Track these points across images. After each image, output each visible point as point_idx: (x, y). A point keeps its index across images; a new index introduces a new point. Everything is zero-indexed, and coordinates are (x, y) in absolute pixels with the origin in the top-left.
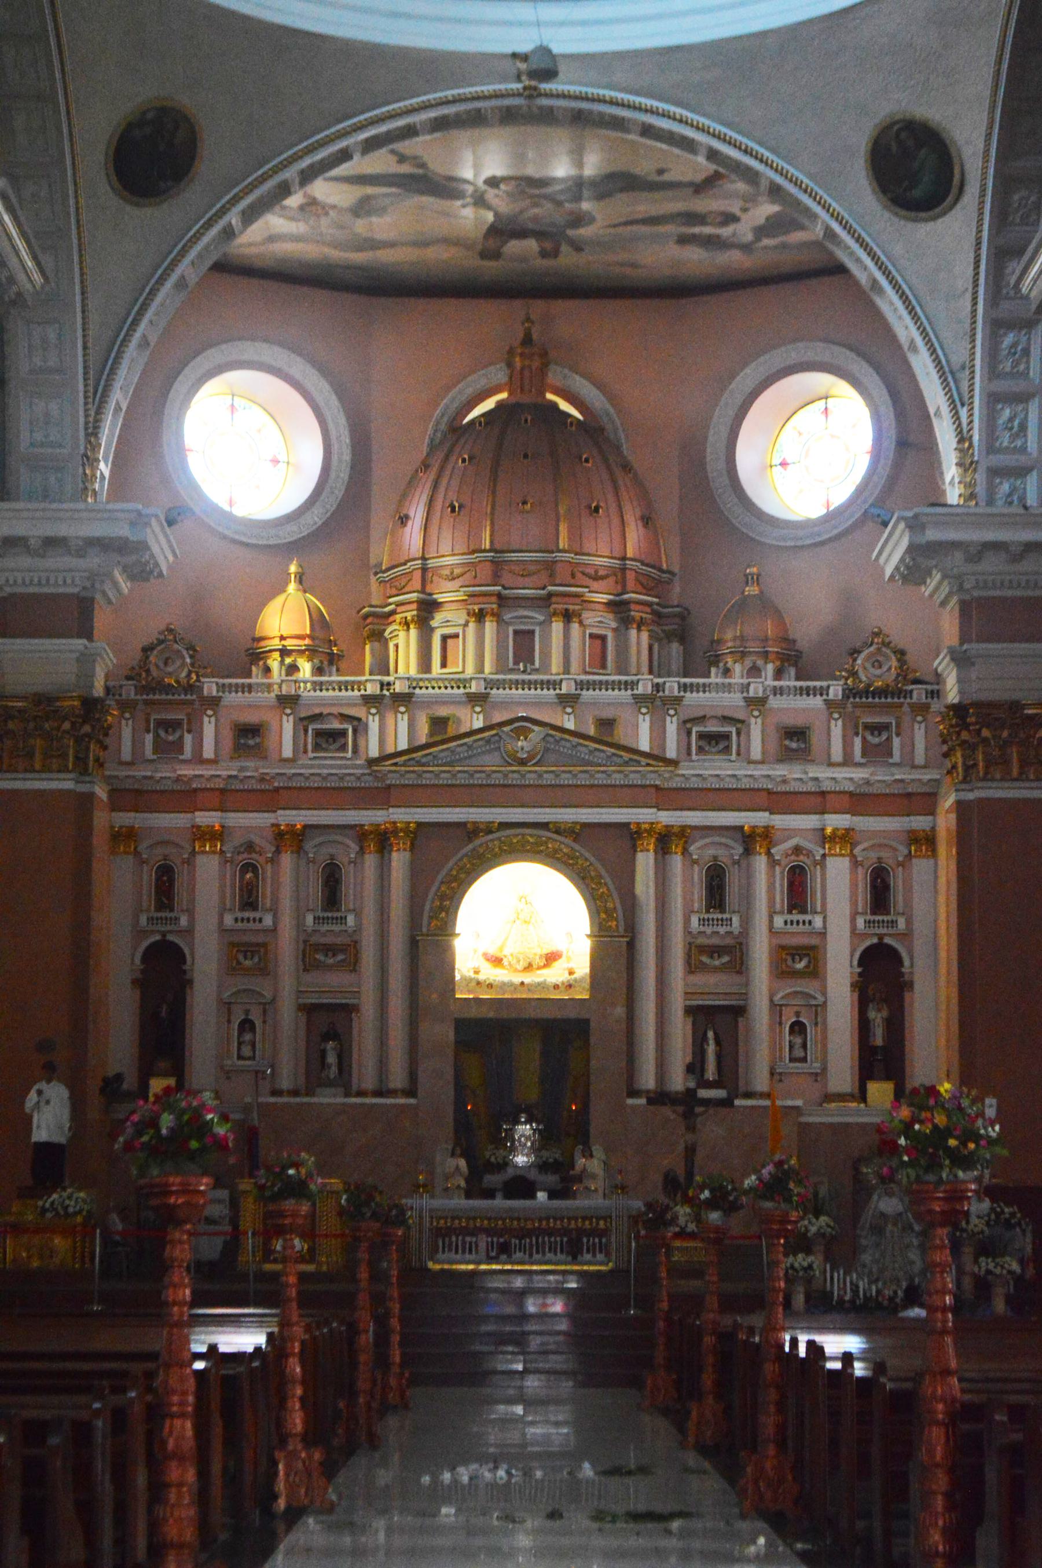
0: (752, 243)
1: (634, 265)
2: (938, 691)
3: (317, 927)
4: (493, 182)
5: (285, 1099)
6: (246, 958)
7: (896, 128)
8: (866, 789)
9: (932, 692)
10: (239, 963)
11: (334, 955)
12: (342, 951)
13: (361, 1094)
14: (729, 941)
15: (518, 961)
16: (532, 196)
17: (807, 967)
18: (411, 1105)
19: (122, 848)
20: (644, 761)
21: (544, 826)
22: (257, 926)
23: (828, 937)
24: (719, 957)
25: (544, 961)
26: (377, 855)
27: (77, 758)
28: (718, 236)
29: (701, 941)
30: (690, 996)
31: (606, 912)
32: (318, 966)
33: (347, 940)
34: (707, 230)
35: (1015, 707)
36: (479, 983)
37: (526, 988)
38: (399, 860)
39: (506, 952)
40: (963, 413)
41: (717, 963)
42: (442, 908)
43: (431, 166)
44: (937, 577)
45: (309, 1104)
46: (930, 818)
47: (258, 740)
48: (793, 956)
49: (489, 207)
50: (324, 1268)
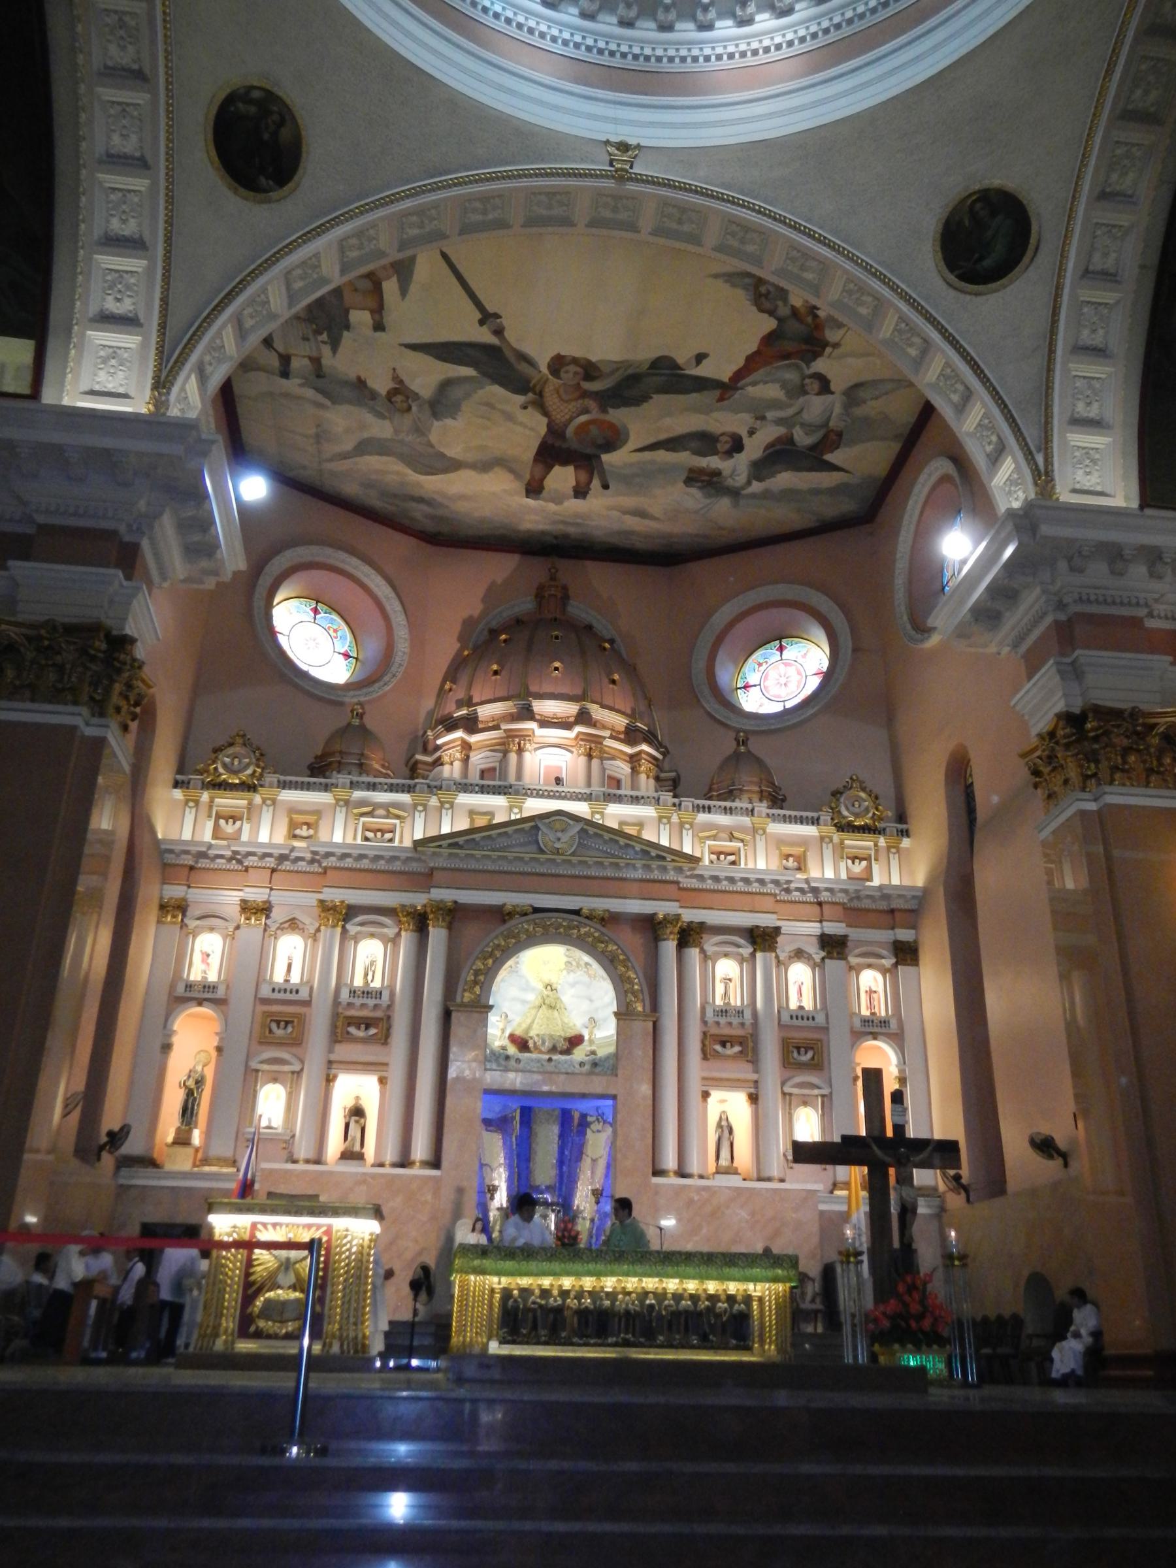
0: (743, 488)
1: (641, 514)
2: (907, 831)
3: (352, 1000)
4: (558, 364)
5: (301, 1167)
6: (278, 1027)
7: (969, 201)
8: (856, 904)
9: (902, 831)
10: (271, 1031)
11: (367, 1028)
13: (382, 1165)
15: (543, 1043)
16: (585, 394)
17: (813, 1058)
18: (434, 1177)
19: (169, 918)
20: (669, 857)
21: (577, 912)
22: (293, 997)
23: (831, 1031)
24: (732, 1046)
25: (566, 1046)
26: (415, 935)
27: (92, 699)
28: (717, 473)
29: (714, 1030)
30: (706, 1083)
31: (634, 993)
34: (713, 462)
35: (1135, 714)
36: (507, 1058)
38: (437, 935)
39: (532, 1033)
40: (1040, 459)
42: (475, 983)
43: (507, 334)
44: (1038, 590)
46: (913, 932)
47: (311, 832)
48: (798, 1048)
49: (546, 413)
50: (336, 1348)
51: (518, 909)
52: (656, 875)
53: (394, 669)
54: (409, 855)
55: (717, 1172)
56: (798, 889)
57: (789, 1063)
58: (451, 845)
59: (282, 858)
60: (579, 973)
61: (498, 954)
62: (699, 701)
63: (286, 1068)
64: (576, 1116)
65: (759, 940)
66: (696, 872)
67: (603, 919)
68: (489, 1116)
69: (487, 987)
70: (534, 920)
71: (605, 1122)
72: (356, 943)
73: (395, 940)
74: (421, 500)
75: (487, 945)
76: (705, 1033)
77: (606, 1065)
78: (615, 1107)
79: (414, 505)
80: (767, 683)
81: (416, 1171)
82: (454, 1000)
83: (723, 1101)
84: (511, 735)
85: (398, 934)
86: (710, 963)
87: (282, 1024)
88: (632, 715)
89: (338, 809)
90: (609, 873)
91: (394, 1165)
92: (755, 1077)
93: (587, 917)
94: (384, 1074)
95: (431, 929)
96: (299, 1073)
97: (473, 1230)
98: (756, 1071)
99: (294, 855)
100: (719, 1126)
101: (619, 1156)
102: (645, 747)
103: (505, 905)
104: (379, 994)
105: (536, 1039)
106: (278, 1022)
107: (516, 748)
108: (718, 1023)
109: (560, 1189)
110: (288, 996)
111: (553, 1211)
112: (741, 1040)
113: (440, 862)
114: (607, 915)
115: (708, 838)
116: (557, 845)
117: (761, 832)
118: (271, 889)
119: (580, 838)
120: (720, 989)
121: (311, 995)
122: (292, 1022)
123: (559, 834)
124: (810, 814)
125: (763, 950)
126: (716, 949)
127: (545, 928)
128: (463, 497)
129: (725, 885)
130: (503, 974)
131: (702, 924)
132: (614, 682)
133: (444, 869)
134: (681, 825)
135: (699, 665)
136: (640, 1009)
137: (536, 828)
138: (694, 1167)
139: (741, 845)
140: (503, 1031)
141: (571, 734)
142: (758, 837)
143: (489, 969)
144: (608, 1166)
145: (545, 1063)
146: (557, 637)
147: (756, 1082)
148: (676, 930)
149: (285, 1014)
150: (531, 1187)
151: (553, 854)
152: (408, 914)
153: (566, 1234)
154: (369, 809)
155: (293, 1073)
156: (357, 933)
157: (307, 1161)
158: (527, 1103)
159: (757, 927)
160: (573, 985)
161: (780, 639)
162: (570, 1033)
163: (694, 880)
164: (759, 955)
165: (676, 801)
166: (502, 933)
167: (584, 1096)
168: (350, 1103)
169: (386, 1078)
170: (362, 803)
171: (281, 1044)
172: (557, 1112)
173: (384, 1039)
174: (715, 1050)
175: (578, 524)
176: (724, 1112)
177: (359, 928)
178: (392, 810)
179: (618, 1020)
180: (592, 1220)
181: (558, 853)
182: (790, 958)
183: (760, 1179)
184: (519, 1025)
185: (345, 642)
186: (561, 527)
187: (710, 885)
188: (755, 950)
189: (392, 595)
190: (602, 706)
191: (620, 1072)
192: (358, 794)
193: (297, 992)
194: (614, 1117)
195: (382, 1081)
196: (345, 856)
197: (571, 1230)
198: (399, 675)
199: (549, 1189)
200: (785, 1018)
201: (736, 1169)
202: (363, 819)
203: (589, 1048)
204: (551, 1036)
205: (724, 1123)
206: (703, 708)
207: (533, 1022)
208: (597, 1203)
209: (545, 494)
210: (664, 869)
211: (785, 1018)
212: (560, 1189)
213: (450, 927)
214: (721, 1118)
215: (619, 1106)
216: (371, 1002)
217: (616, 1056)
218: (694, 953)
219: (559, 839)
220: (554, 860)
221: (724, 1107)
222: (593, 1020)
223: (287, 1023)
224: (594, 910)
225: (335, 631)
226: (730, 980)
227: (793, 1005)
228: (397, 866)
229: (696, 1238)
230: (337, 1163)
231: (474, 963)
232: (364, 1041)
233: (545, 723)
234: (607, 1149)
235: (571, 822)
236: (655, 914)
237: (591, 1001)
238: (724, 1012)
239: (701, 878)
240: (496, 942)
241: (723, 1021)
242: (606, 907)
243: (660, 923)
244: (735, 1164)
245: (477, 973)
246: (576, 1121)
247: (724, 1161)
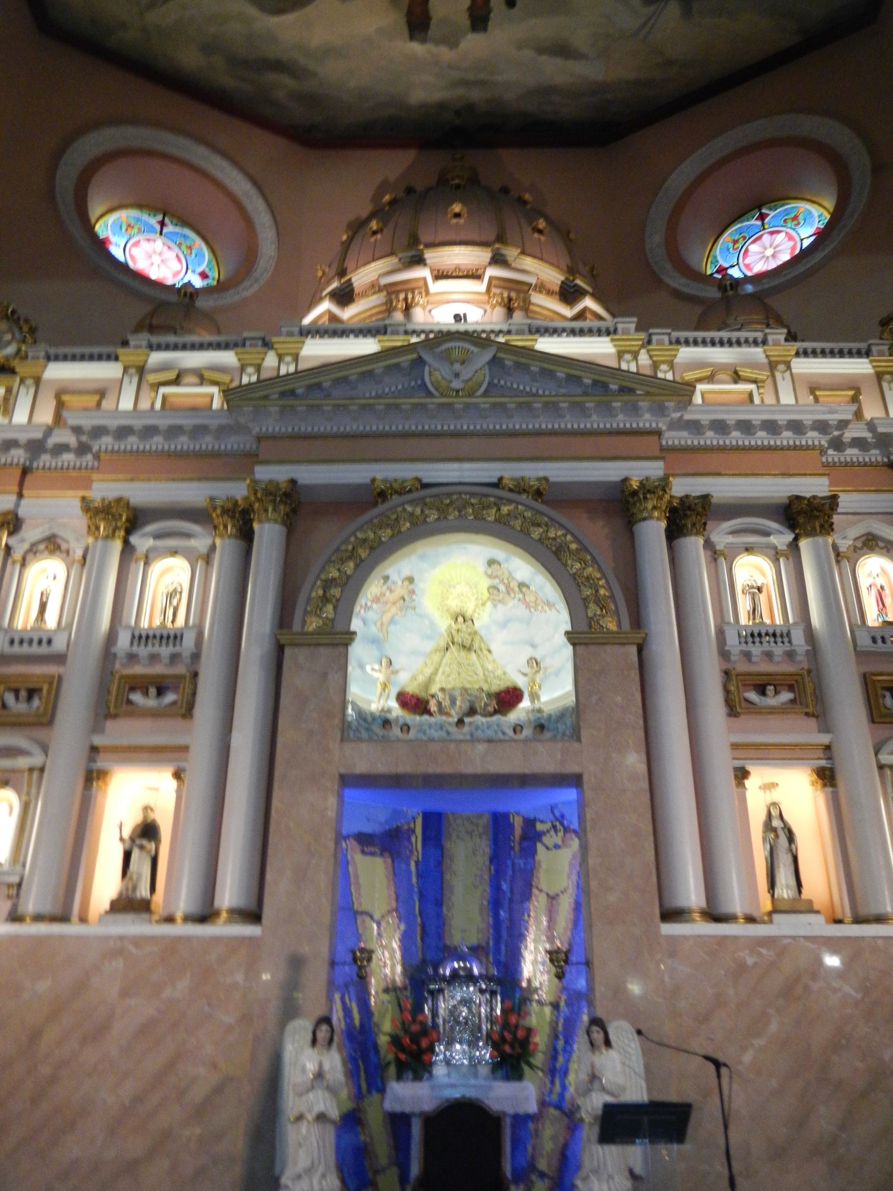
3: (135, 648)
6: (17, 698)
11: (160, 692)
12: (176, 689)
13: (170, 919)
14: (787, 668)
15: (453, 702)
18: (251, 940)
22: (44, 650)
24: (777, 692)
29: (742, 667)
30: (740, 753)
31: (598, 601)
32: (128, 710)
33: (180, 669)
36: (386, 723)
37: (466, 729)
39: (434, 689)
41: (772, 701)
42: (325, 599)
45: (62, 938)
51: (396, 486)
52: (622, 421)
53: (256, 274)
54: (224, 421)
55: (775, 911)
56: (859, 443)
57: (885, 716)
58: (283, 394)
59: (36, 447)
60: (511, 604)
61: (363, 553)
62: (660, 281)
63: (23, 762)
64: (518, 823)
65: (801, 520)
66: (687, 417)
67: (538, 494)
68: (367, 828)
69: (346, 608)
70: (423, 499)
71: (566, 830)
72: (147, 564)
73: (208, 559)
74: (279, 66)
75: (346, 541)
76: (727, 673)
77: (561, 727)
78: (582, 804)
79: (271, 77)
80: (747, 261)
81: (220, 929)
82: (290, 626)
83: (772, 786)
84: (392, 290)
85: (213, 548)
86: (722, 560)
87: (23, 694)
88: (571, 271)
89: (126, 380)
90: (545, 423)
91: (187, 919)
92: (825, 739)
93: (511, 490)
94: (183, 764)
95: (256, 526)
96: (42, 770)
97: (314, 1042)
98: (826, 728)
99: (51, 441)
100: (768, 826)
101: (594, 884)
102: (588, 302)
103: (373, 480)
104: (176, 638)
105: (440, 696)
106: (16, 692)
107: (401, 305)
108: (747, 655)
109: (497, 950)
110: (35, 649)
111: (482, 991)
112: (792, 683)
113: (271, 424)
114: (544, 486)
115: (700, 380)
116: (456, 384)
117: (782, 367)
118: (20, 495)
119: (492, 378)
120: (744, 604)
121: (68, 646)
122: (40, 690)
123: (457, 367)
124: (854, 346)
125: (811, 533)
126: (730, 539)
127: (443, 513)
128: (328, 52)
129: (736, 437)
130: (373, 588)
131: (706, 498)
132: (540, 232)
133: (274, 437)
134: (655, 366)
135: (655, 239)
136: (612, 626)
137: (420, 362)
138: (736, 904)
139: (752, 387)
140: (385, 686)
141: (482, 287)
142: (778, 375)
143: (348, 577)
144: (577, 907)
145: (453, 730)
146: (458, 187)
147: (828, 748)
148: (663, 504)
149: (25, 677)
150: (446, 948)
151: (446, 396)
152: (225, 511)
153: (508, 1036)
154: (172, 375)
155: (31, 770)
156: (148, 551)
157: (38, 918)
158: (435, 804)
159: (798, 498)
160: (504, 625)
161: (759, 207)
162: (497, 686)
163: (685, 434)
164: (804, 544)
165: (642, 336)
166: (370, 521)
167: (525, 781)
168: (131, 820)
169: (184, 770)
170: (163, 368)
171: (18, 724)
172: (486, 819)
173: (187, 710)
174: (746, 700)
175: (482, 83)
176: (774, 804)
177: (150, 542)
178: (208, 375)
179: (574, 645)
180: (555, 1006)
181: (457, 395)
182: (855, 549)
183: (858, 920)
184: (414, 678)
185: (205, 260)
186: (461, 91)
187: (710, 438)
188: (796, 539)
189: (253, 192)
190: (523, 253)
191: (585, 734)
192: (156, 358)
193: (50, 642)
194: (581, 818)
195: (177, 775)
196: (123, 432)
197: (517, 1027)
198: (262, 282)
199: (476, 951)
200: (864, 641)
201: (810, 902)
202: (163, 390)
203: (531, 708)
204: (465, 690)
205: (776, 823)
206: (668, 286)
207: (436, 672)
208: (560, 976)
209: (433, 31)
210: (635, 410)
211: (864, 641)
212: (497, 950)
213: (290, 523)
214: (769, 816)
215: (589, 794)
216: (165, 651)
217: (578, 710)
218: (694, 545)
219: (457, 375)
220: (450, 405)
221: (773, 795)
222: (534, 662)
223: (32, 693)
224: (523, 478)
225: (190, 248)
226: (759, 589)
227: (873, 619)
228: (208, 443)
229: (760, 1042)
230: (101, 919)
231: (323, 569)
232: (154, 714)
233: (440, 276)
234: (574, 877)
235: (475, 350)
236: (626, 480)
237: (533, 646)
238: (755, 636)
239: (695, 427)
240: (360, 535)
241: (756, 650)
242: (541, 474)
243: (634, 493)
244: (805, 895)
245: (328, 584)
246: (518, 832)
247: (785, 891)
